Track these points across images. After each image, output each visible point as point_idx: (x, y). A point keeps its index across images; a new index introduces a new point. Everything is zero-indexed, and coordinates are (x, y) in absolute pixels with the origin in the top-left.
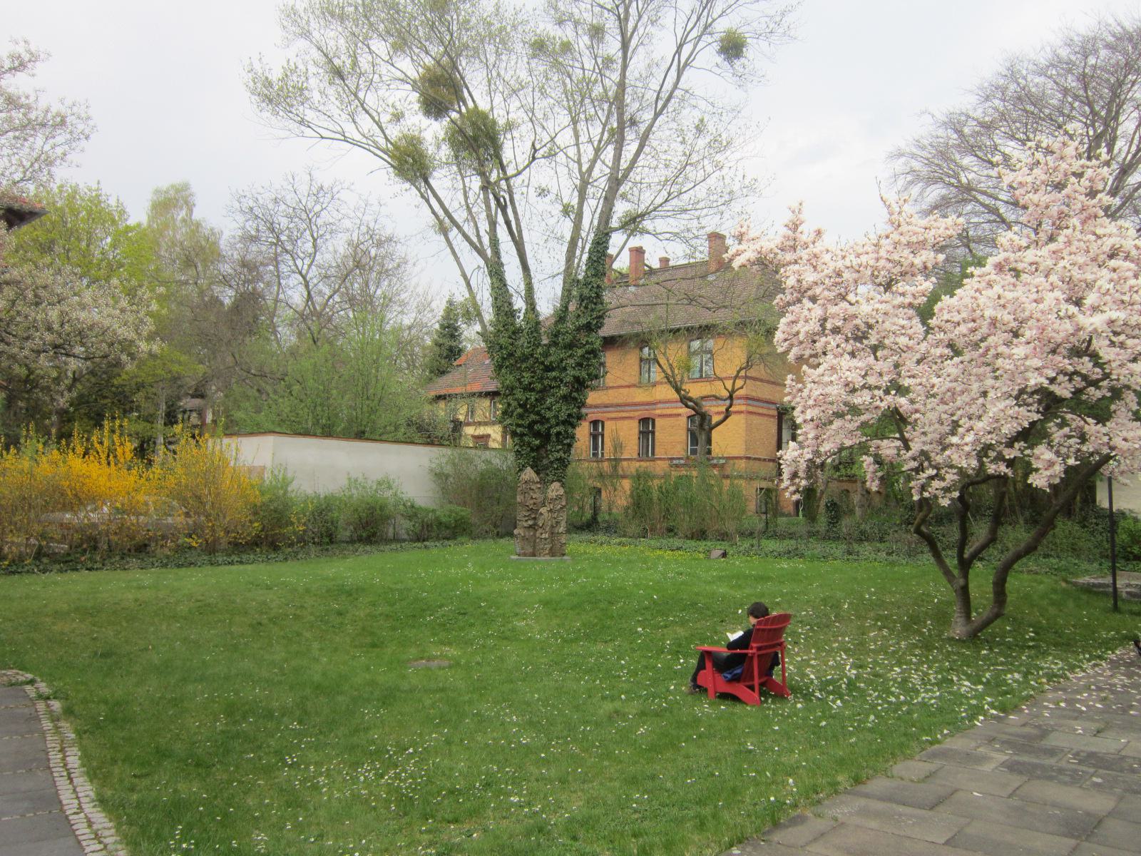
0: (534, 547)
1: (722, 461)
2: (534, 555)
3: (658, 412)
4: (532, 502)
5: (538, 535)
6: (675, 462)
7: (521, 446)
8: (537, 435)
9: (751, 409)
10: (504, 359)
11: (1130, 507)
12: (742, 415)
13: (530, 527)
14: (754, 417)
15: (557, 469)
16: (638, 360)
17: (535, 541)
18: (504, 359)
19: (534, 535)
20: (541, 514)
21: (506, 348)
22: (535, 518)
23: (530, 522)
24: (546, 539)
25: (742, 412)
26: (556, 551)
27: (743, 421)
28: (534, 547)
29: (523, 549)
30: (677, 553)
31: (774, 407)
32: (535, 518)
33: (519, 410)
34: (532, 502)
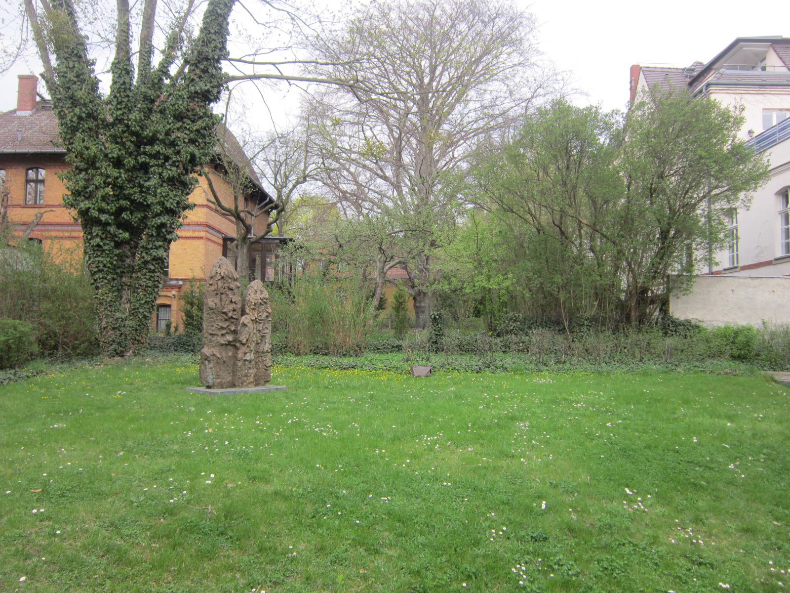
0: (234, 373)
1: (180, 283)
2: (233, 385)
3: (47, 234)
4: (231, 307)
5: (240, 355)
6: (735, 246)
7: (102, 239)
8: (125, 226)
9: (209, 236)
10: (80, 118)
11: (695, 316)
12: (202, 241)
13: (229, 344)
14: (210, 244)
15: (154, 271)
16: (23, 180)
17: (235, 364)
18: (80, 118)
19: (235, 357)
20: (244, 325)
21: (85, 105)
22: (235, 332)
23: (230, 338)
24: (250, 361)
25: (202, 238)
26: (262, 379)
27: (202, 247)
28: (234, 373)
29: (218, 376)
30: (350, 372)
31: (220, 236)
32: (235, 332)
33: (109, 190)
34: (231, 307)
